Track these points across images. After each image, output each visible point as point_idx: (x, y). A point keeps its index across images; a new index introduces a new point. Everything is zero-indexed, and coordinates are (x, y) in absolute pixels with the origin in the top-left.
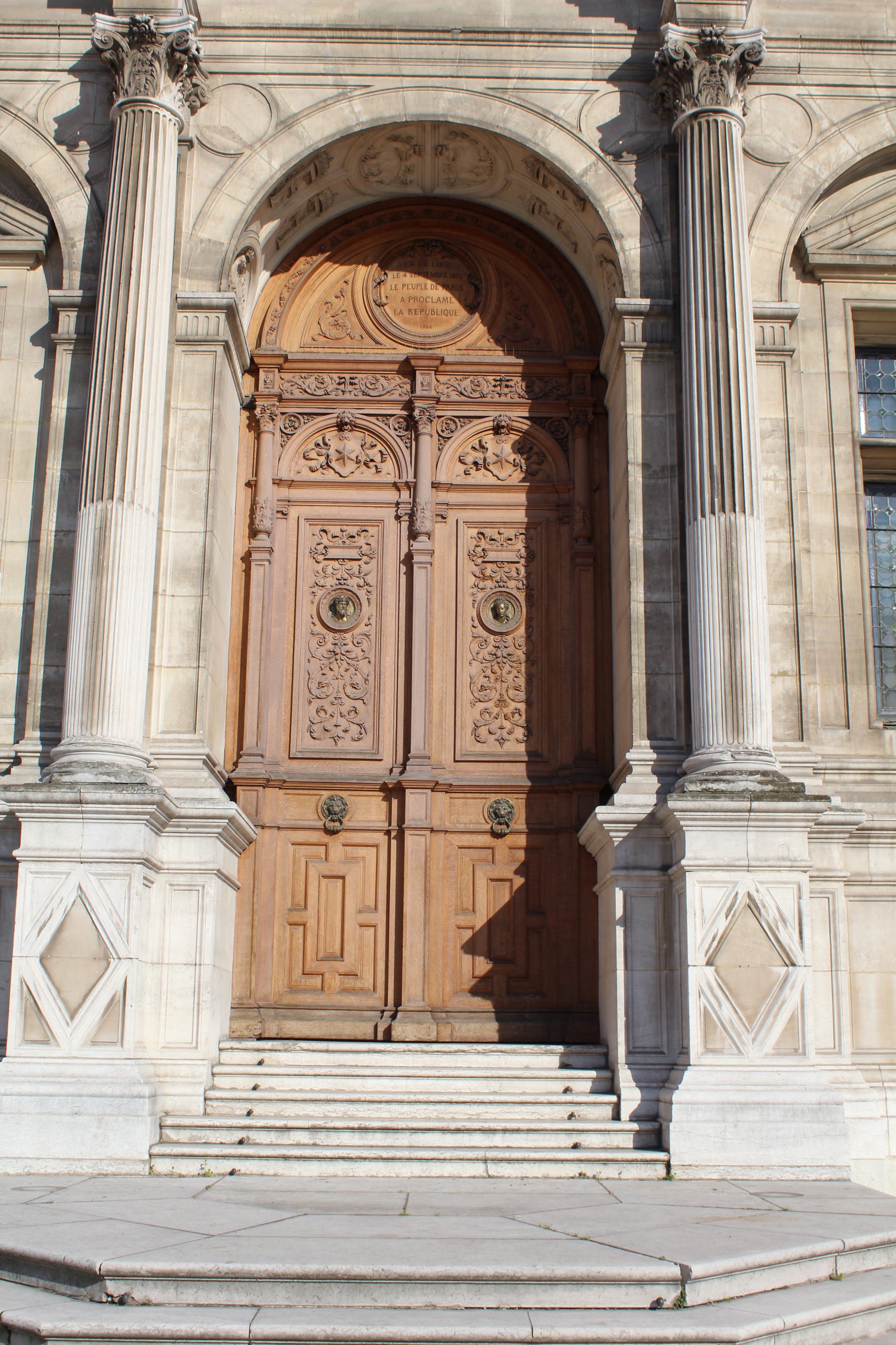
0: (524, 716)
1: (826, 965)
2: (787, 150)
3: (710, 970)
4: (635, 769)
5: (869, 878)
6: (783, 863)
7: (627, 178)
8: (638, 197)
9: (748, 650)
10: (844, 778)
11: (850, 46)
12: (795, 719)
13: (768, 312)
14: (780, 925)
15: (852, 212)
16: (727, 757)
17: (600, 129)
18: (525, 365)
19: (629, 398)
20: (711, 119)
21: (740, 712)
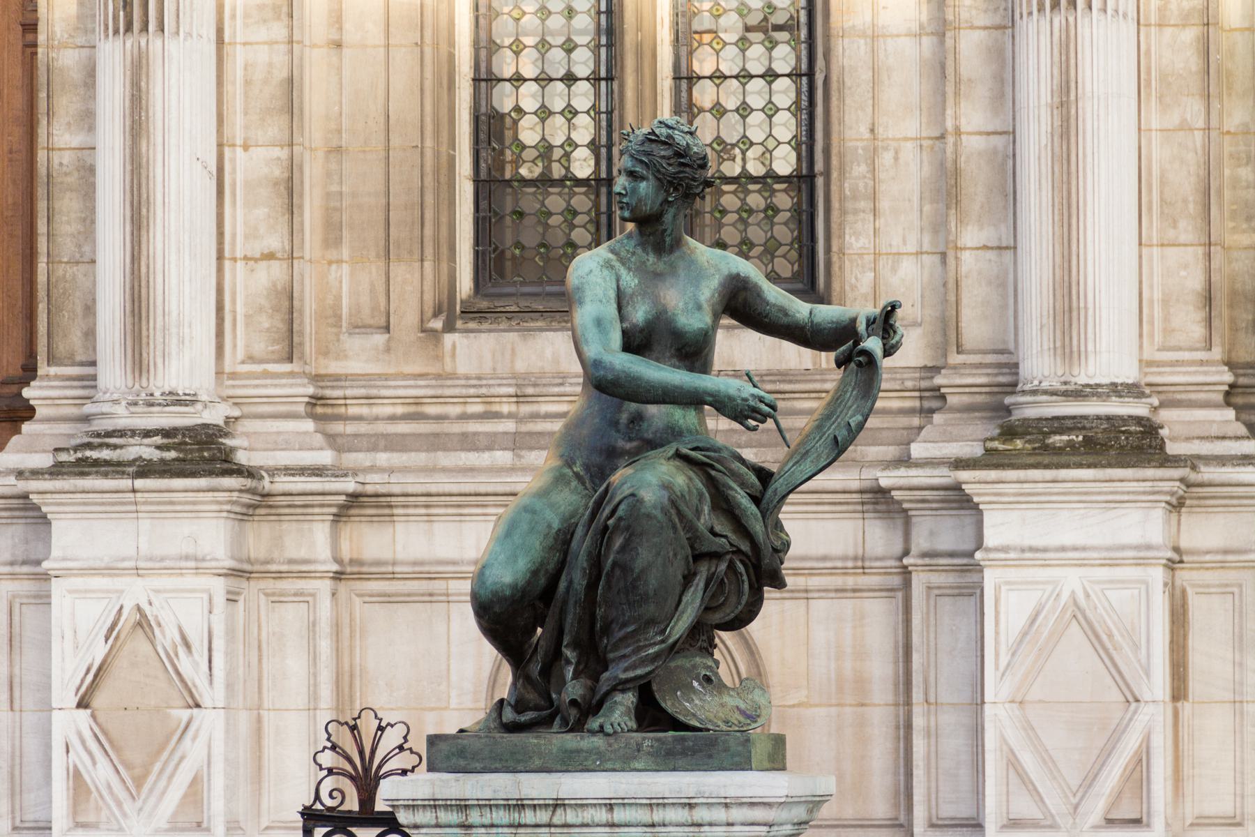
1: (301, 701)
3: (84, 714)
4: (41, 412)
5: (390, 569)
6: (183, 564)
9: (159, 246)
12: (283, 327)
14: (181, 651)
21: (144, 340)
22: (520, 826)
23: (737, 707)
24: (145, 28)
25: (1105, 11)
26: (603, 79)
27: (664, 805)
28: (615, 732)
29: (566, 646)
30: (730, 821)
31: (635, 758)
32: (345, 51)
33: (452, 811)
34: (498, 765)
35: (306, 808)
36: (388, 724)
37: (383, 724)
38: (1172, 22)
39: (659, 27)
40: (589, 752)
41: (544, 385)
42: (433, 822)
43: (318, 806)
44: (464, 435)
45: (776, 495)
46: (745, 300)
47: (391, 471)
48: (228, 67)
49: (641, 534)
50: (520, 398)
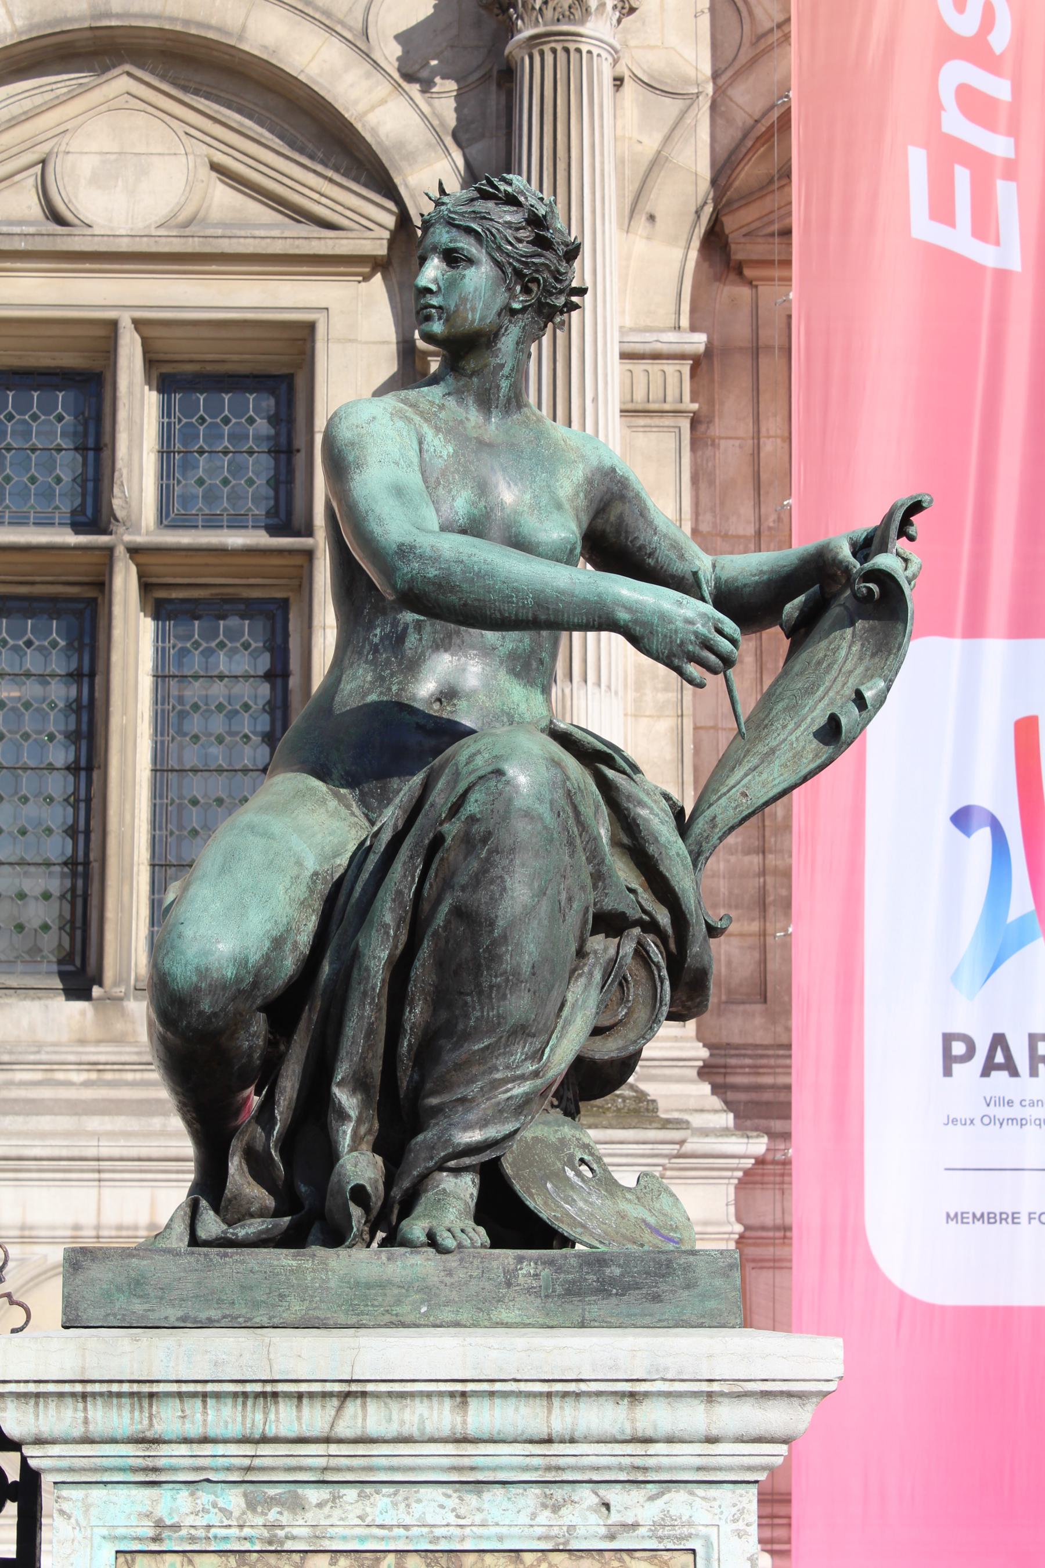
22: (264, 1440)
23: (644, 1221)
25: (599, 684)
26: (83, 769)
28: (460, 1246)
29: (339, 1084)
30: (714, 1432)
33: (120, 1407)
34: (214, 1314)
38: (647, 713)
39: (139, 721)
40: (406, 1286)
41: (20, 1053)
42: (78, 1432)
45: (714, 826)
46: (621, 517)
49: (512, 850)
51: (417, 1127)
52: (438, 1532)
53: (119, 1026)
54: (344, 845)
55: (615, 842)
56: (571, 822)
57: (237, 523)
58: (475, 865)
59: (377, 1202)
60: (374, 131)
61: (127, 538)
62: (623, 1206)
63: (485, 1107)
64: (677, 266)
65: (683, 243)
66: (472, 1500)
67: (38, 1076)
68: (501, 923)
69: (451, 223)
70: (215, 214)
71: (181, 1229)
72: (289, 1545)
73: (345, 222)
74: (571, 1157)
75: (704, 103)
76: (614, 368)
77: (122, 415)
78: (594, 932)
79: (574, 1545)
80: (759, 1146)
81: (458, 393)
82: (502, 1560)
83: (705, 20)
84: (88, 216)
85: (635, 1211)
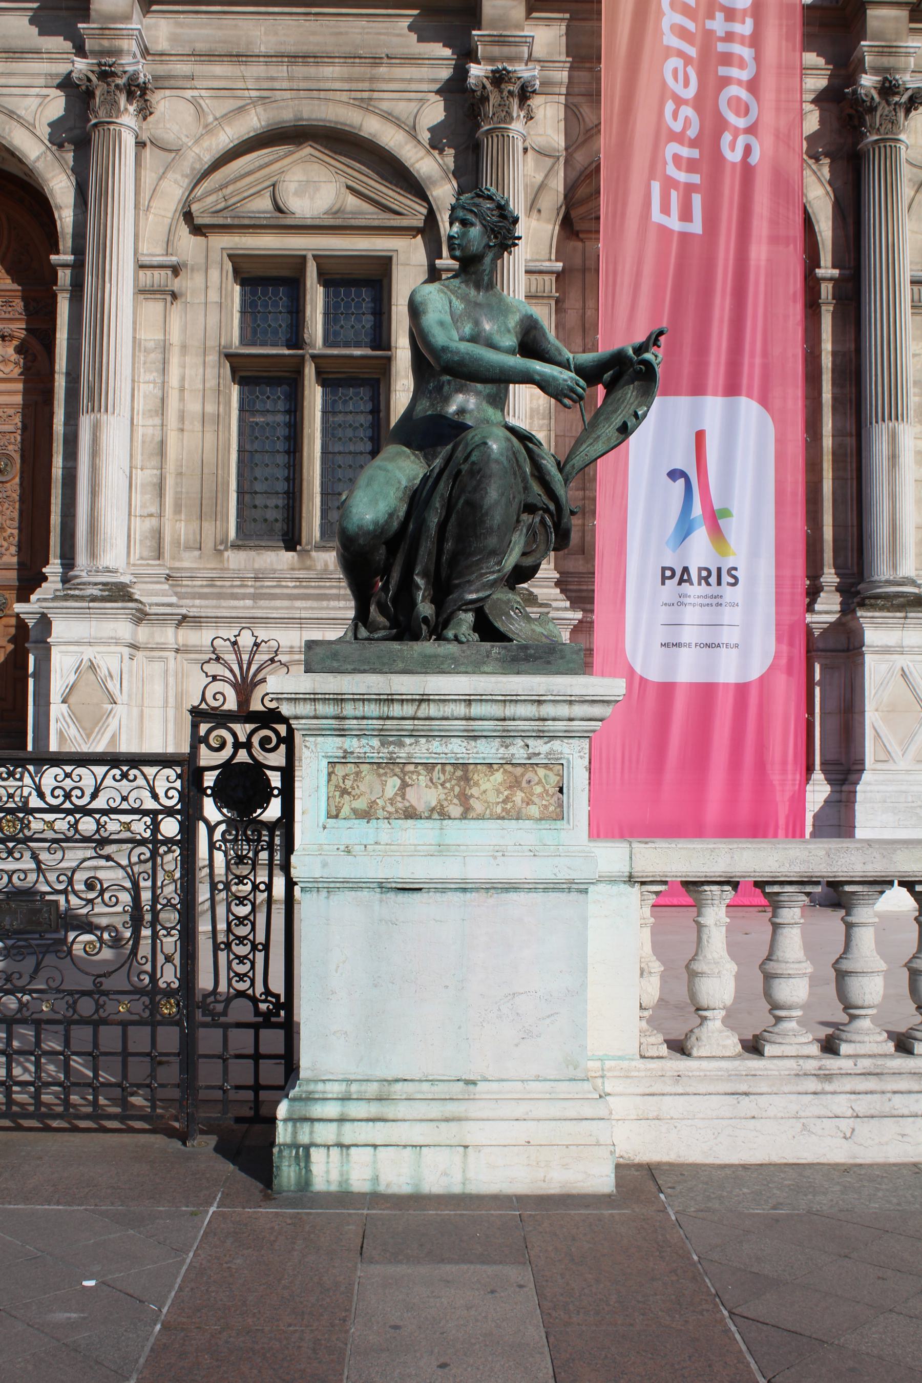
0: (17, 539)
1: (161, 704)
2: (180, 139)
4: (50, 579)
7: (67, 164)
8: (73, 179)
10: (195, 583)
11: (229, 59)
12: (156, 545)
13: (155, 263)
15: (226, 186)
16: (84, 574)
17: (50, 125)
18: (23, 291)
19: (58, 327)
20: (105, 128)
22: (388, 718)
24: (100, 410)
27: (516, 701)
28: (468, 641)
29: (417, 575)
30: (572, 716)
31: (484, 663)
32: (185, 433)
33: (329, 704)
34: (366, 667)
35: (194, 707)
36: (263, 641)
37: (259, 641)
40: (445, 657)
42: (312, 714)
43: (203, 706)
44: (232, 594)
46: (535, 337)
47: (201, 607)
48: (135, 434)
49: (490, 476)
50: (256, 579)
51: (449, 592)
52: (458, 756)
53: (308, 563)
54: (418, 475)
55: (532, 475)
56: (515, 464)
57: (358, 345)
58: (474, 483)
59: (432, 623)
60: (418, 172)
61: (310, 351)
62: (534, 627)
63: (478, 584)
64: (550, 232)
65: (553, 222)
66: (473, 743)
67: (275, 584)
68: (485, 507)
69: (463, 208)
70: (349, 208)
71: (350, 634)
72: (398, 761)
73: (405, 212)
74: (512, 606)
75: (562, 160)
76: (522, 277)
77: (308, 297)
78: (523, 512)
79: (514, 761)
80: (579, 615)
81: (466, 282)
82: (484, 768)
83: (562, 124)
84: (293, 209)
85: (539, 629)
